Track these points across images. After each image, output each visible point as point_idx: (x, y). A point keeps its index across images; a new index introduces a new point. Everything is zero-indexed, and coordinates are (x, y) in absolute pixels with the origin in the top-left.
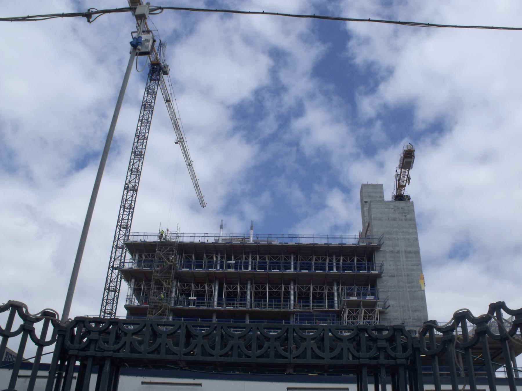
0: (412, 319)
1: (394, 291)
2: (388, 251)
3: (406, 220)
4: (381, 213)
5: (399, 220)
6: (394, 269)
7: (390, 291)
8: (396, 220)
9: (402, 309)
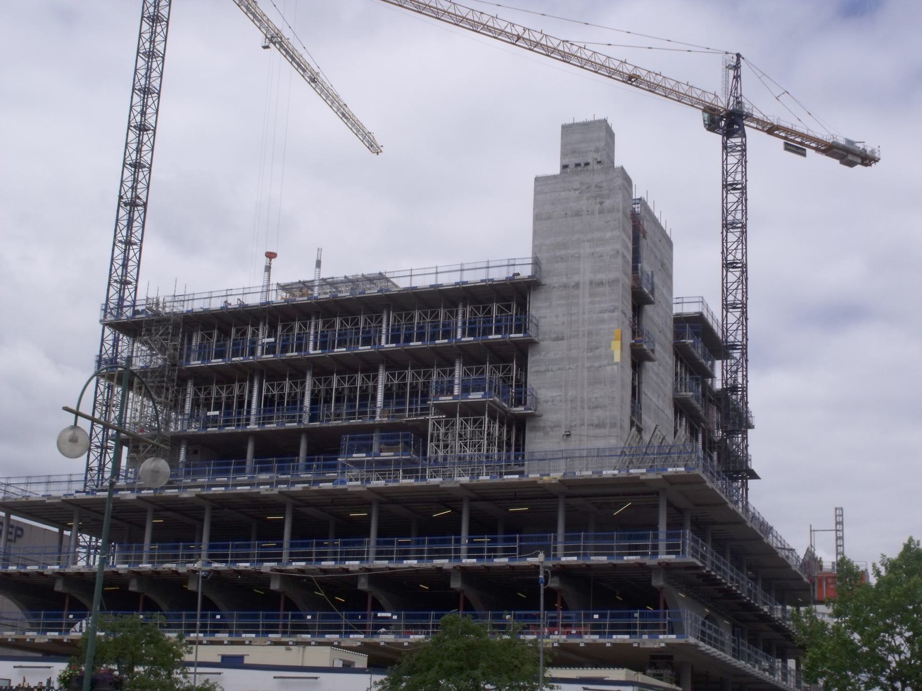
0: (588, 425)
2: (556, 285)
3: (601, 212)
4: (553, 204)
5: (587, 215)
6: (563, 323)
7: (552, 370)
8: (581, 215)
9: (569, 406)
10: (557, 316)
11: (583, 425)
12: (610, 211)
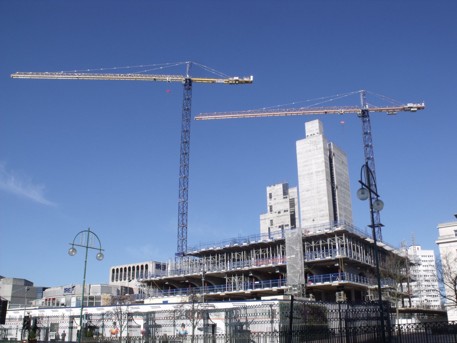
1: (309, 200)
2: (306, 174)
3: (317, 149)
7: (307, 201)
9: (313, 211)
10: (307, 184)
11: (318, 217)
12: (320, 148)
